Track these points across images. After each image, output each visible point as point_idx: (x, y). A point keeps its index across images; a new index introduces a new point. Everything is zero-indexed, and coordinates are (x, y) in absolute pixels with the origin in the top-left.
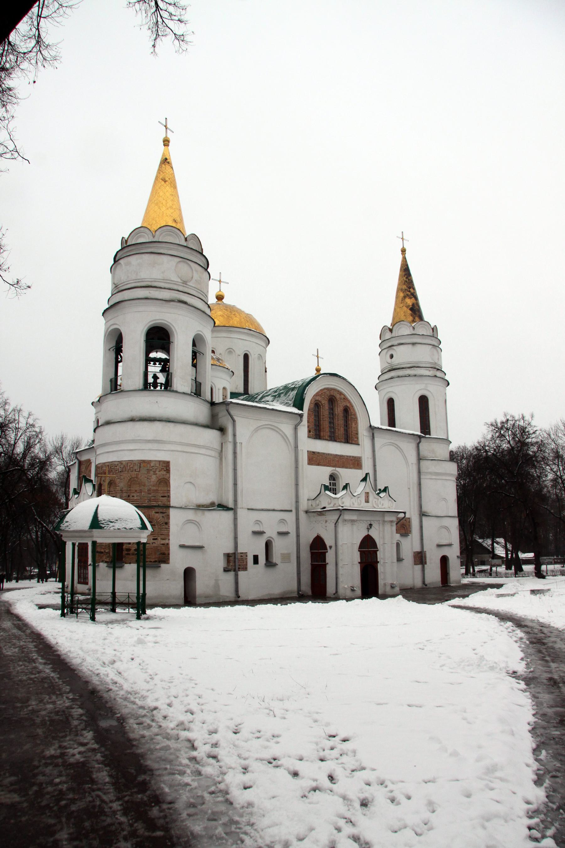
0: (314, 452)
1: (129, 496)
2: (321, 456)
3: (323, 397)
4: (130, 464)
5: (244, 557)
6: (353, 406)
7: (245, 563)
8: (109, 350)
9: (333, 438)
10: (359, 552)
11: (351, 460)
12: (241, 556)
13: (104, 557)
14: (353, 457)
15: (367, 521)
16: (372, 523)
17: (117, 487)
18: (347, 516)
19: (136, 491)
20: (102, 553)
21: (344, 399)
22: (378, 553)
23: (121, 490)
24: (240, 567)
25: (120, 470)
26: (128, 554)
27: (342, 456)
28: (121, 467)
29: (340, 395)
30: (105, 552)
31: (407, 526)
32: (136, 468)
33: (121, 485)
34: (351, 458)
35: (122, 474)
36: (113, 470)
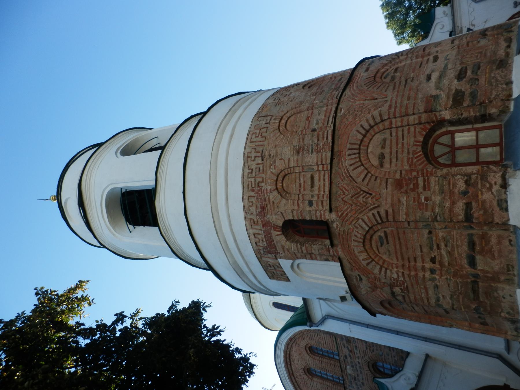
1: (314, 130)
4: (254, 137)
8: (131, 232)
13: (486, 196)
17: (292, 165)
19: (308, 119)
20: (468, 205)
23: (298, 153)
25: (259, 160)
26: (473, 95)
28: (255, 157)
30: (465, 193)
32: (264, 122)
33: (287, 151)
35: (267, 154)
36: (258, 180)
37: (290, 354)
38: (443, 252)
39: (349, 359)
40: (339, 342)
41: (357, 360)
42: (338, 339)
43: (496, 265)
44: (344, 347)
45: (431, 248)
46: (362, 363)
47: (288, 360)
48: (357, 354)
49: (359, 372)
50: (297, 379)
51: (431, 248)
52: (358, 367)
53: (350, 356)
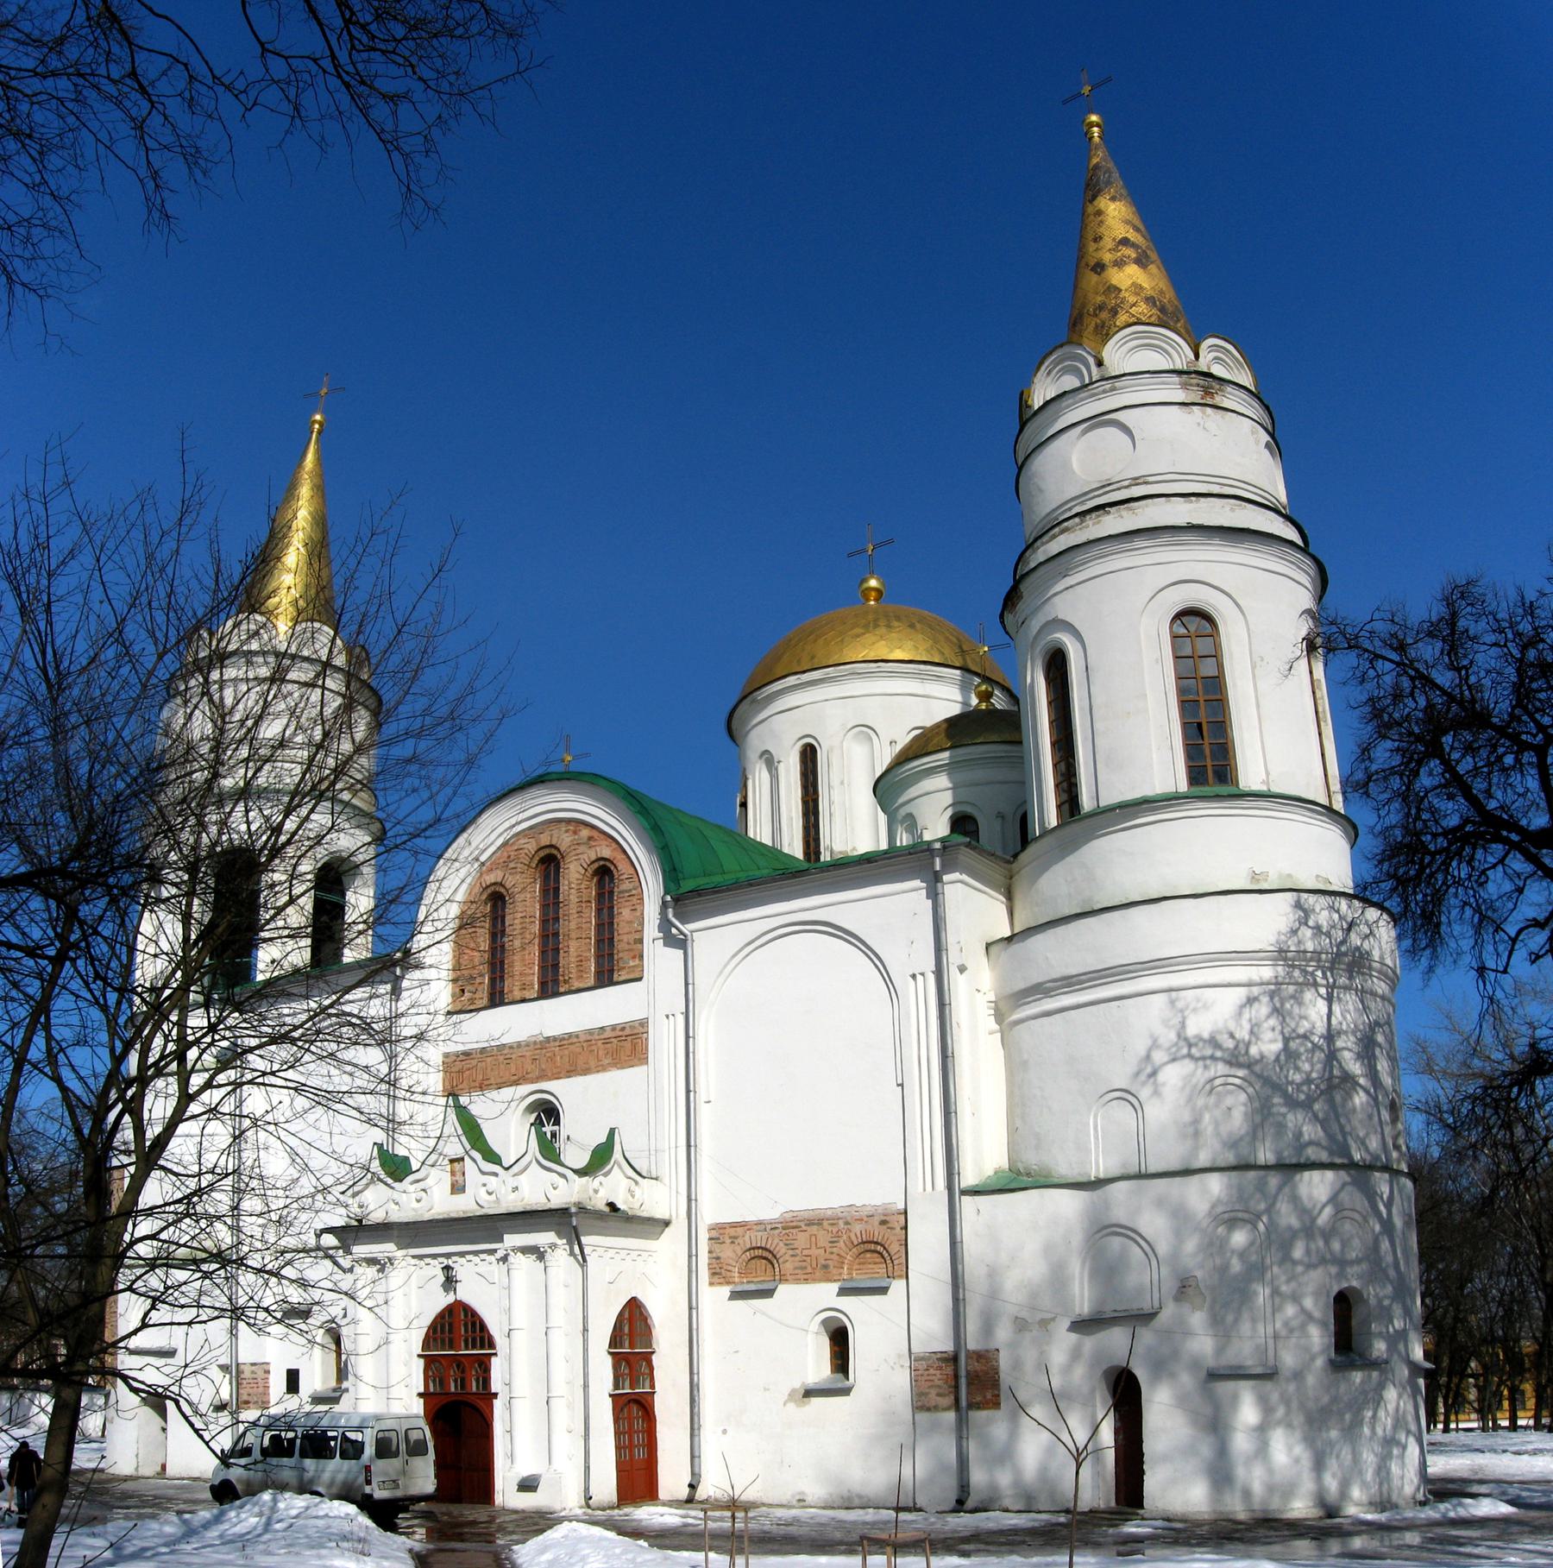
0: (467, 1054)
2: (489, 1059)
3: (512, 865)
5: (260, 1374)
6: (624, 852)
7: (261, 1390)
9: (550, 987)
10: (422, 1362)
11: (607, 1041)
12: (253, 1372)
14: (614, 1028)
15: (434, 1256)
16: (450, 1262)
18: (360, 1250)
21: (590, 838)
22: (493, 1359)
24: (250, 1399)
27: (570, 1035)
29: (575, 833)
31: (894, 1248)
34: (608, 1034)
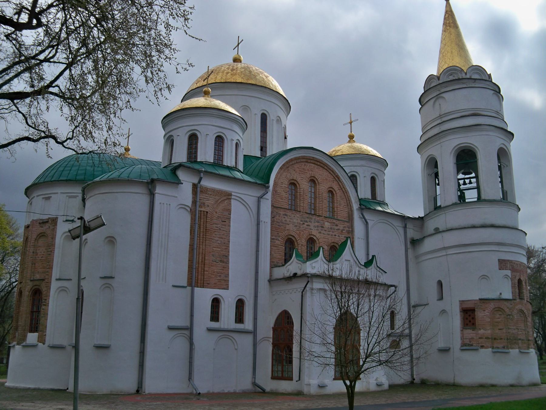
37: (324, 168)
38: (520, 332)
39: (336, 228)
40: (346, 224)
41: (337, 235)
42: (348, 224)
43: (520, 345)
44: (344, 227)
45: (521, 329)
46: (335, 238)
47: (318, 164)
48: (341, 236)
49: (329, 233)
50: (303, 163)
51: (521, 329)
52: (331, 233)
53: (338, 229)
